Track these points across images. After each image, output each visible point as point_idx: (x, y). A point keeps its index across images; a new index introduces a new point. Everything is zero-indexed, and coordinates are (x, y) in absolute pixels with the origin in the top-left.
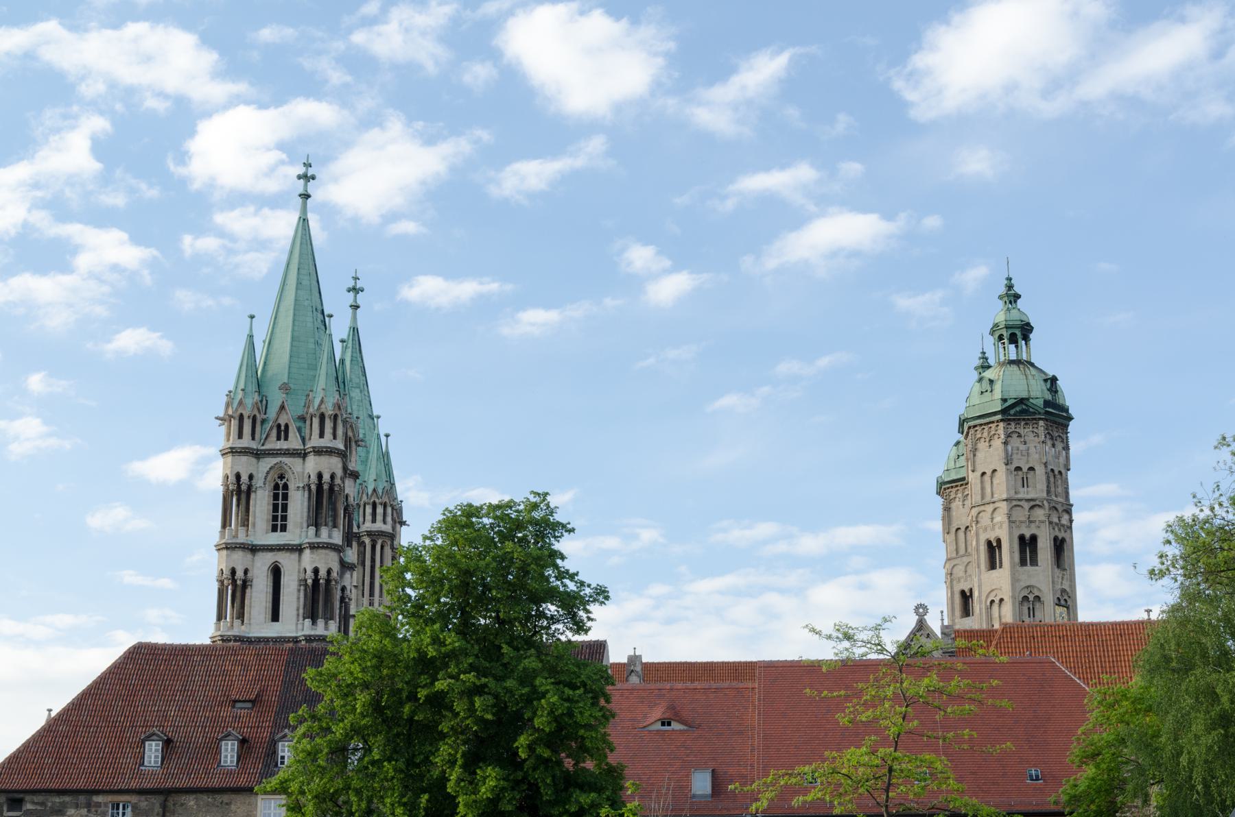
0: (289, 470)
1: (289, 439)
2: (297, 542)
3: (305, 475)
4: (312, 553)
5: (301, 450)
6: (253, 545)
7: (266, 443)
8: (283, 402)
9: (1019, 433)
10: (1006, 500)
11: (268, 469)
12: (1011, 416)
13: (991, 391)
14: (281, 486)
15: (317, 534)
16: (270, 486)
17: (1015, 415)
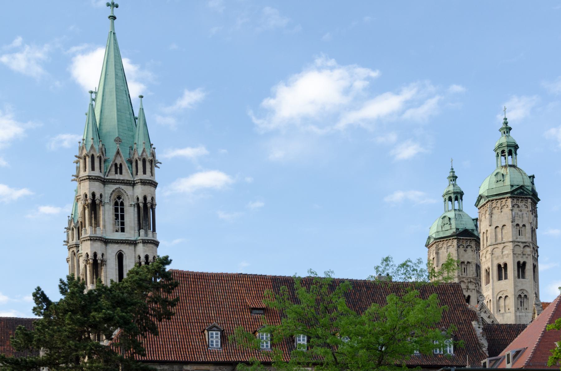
0: (125, 194)
1: (123, 173)
2: (133, 239)
3: (135, 197)
4: (144, 246)
5: (132, 181)
6: (106, 239)
7: (109, 175)
8: (118, 149)
9: (518, 205)
10: (512, 242)
11: (111, 191)
12: (515, 195)
13: (503, 181)
14: (119, 203)
15: (146, 234)
16: (113, 203)
17: (517, 195)
